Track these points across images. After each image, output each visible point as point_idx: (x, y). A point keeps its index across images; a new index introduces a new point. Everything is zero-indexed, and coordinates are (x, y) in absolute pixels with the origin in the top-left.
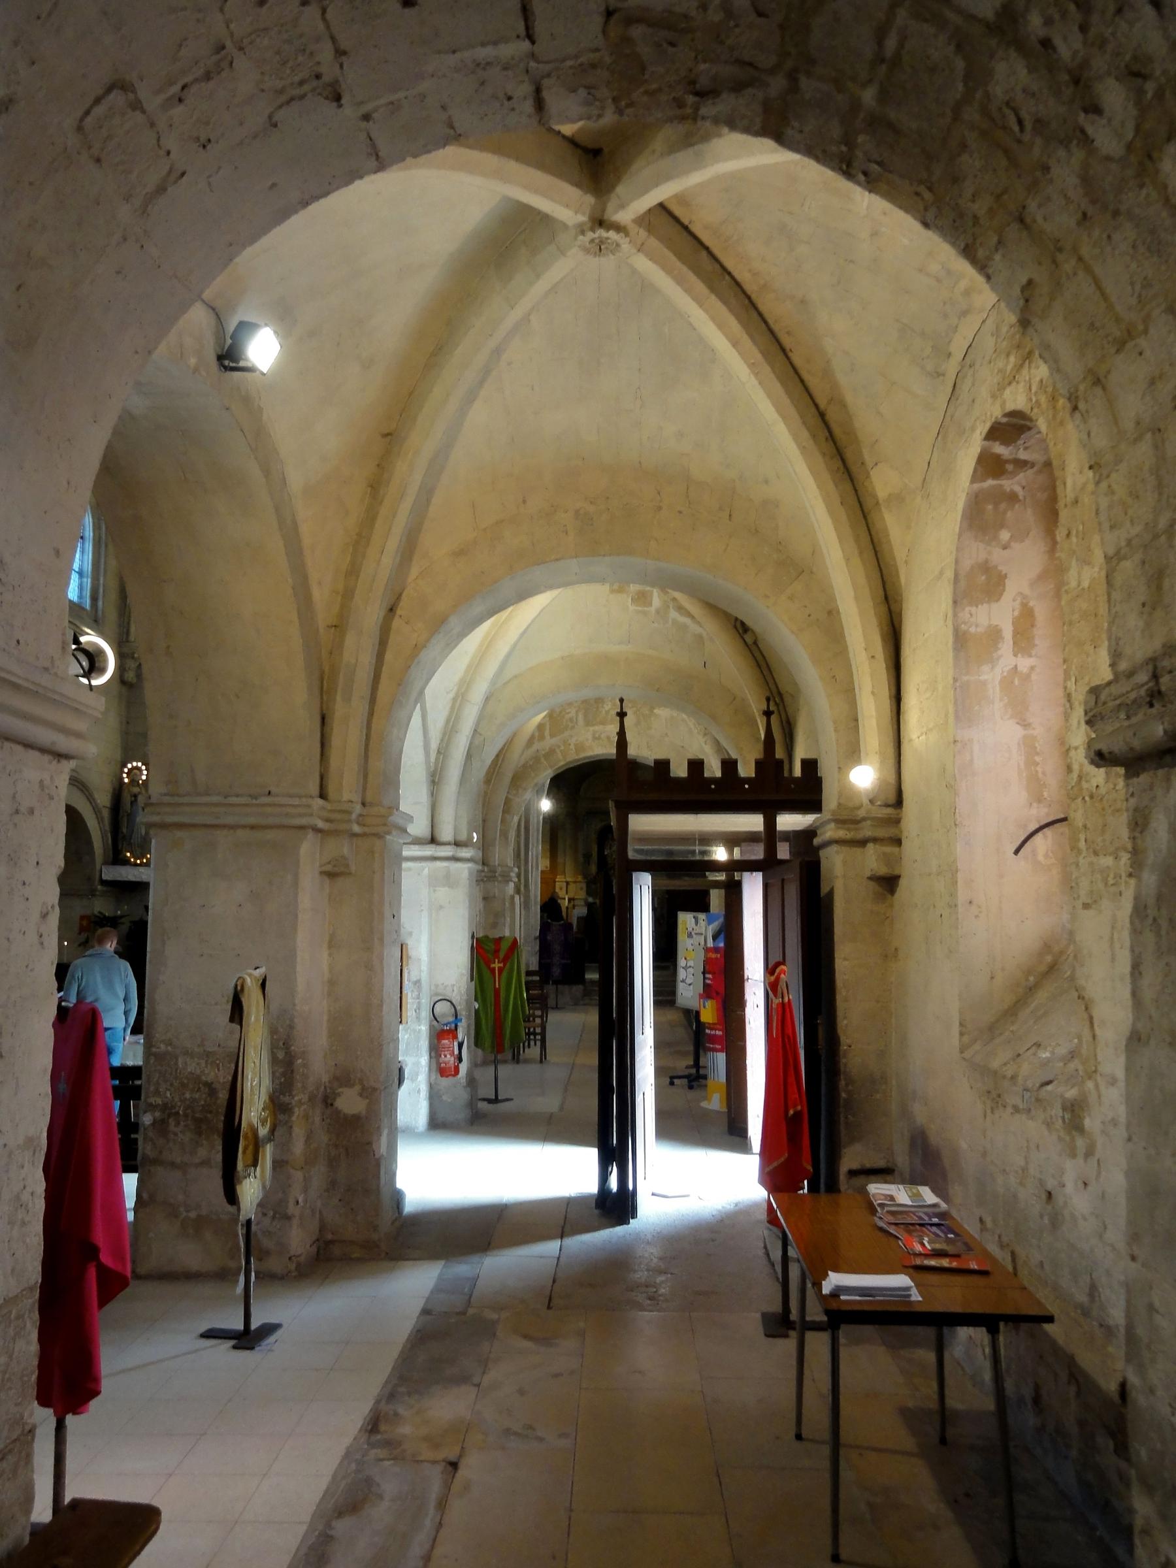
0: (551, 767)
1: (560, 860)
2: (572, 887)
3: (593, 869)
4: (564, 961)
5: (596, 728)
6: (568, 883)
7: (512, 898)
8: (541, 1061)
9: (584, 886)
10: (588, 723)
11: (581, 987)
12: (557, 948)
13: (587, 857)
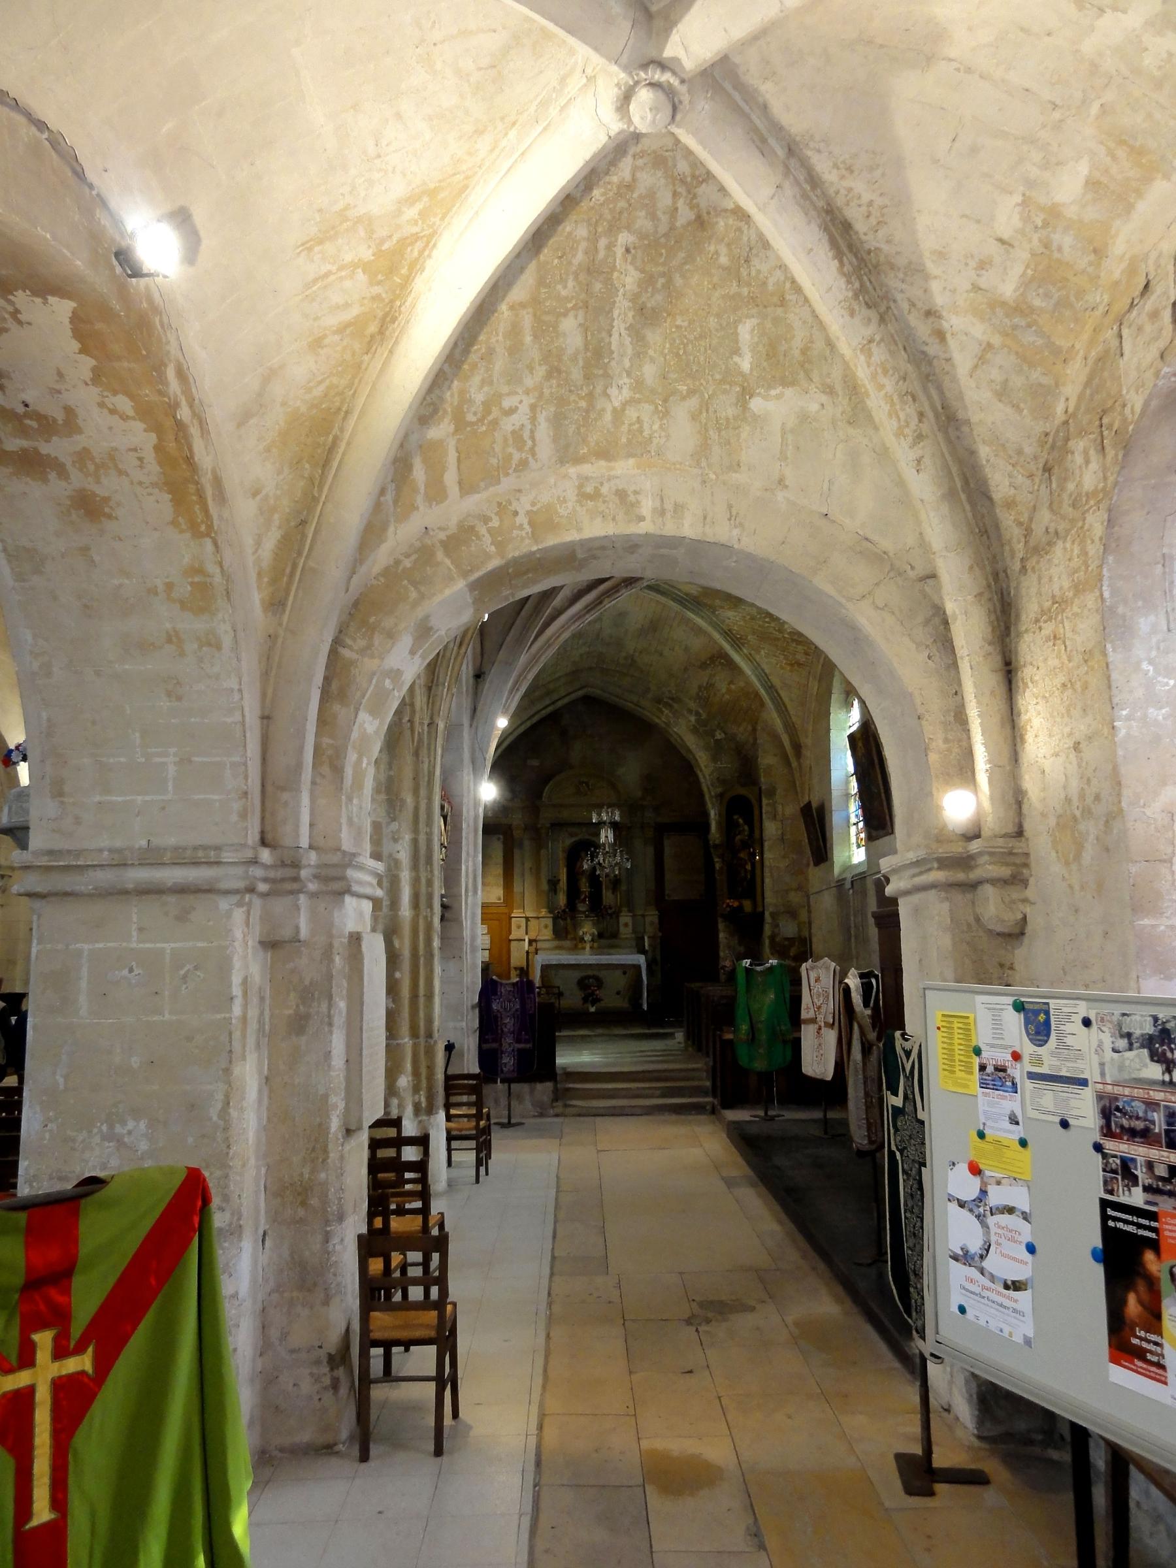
0: (465, 574)
1: (517, 888)
2: (533, 923)
3: (562, 899)
5: (586, 469)
6: (527, 919)
7: (356, 939)
8: (439, 1452)
9: (549, 922)
10: (566, 455)
11: (549, 1085)
12: (509, 1023)
13: (553, 884)
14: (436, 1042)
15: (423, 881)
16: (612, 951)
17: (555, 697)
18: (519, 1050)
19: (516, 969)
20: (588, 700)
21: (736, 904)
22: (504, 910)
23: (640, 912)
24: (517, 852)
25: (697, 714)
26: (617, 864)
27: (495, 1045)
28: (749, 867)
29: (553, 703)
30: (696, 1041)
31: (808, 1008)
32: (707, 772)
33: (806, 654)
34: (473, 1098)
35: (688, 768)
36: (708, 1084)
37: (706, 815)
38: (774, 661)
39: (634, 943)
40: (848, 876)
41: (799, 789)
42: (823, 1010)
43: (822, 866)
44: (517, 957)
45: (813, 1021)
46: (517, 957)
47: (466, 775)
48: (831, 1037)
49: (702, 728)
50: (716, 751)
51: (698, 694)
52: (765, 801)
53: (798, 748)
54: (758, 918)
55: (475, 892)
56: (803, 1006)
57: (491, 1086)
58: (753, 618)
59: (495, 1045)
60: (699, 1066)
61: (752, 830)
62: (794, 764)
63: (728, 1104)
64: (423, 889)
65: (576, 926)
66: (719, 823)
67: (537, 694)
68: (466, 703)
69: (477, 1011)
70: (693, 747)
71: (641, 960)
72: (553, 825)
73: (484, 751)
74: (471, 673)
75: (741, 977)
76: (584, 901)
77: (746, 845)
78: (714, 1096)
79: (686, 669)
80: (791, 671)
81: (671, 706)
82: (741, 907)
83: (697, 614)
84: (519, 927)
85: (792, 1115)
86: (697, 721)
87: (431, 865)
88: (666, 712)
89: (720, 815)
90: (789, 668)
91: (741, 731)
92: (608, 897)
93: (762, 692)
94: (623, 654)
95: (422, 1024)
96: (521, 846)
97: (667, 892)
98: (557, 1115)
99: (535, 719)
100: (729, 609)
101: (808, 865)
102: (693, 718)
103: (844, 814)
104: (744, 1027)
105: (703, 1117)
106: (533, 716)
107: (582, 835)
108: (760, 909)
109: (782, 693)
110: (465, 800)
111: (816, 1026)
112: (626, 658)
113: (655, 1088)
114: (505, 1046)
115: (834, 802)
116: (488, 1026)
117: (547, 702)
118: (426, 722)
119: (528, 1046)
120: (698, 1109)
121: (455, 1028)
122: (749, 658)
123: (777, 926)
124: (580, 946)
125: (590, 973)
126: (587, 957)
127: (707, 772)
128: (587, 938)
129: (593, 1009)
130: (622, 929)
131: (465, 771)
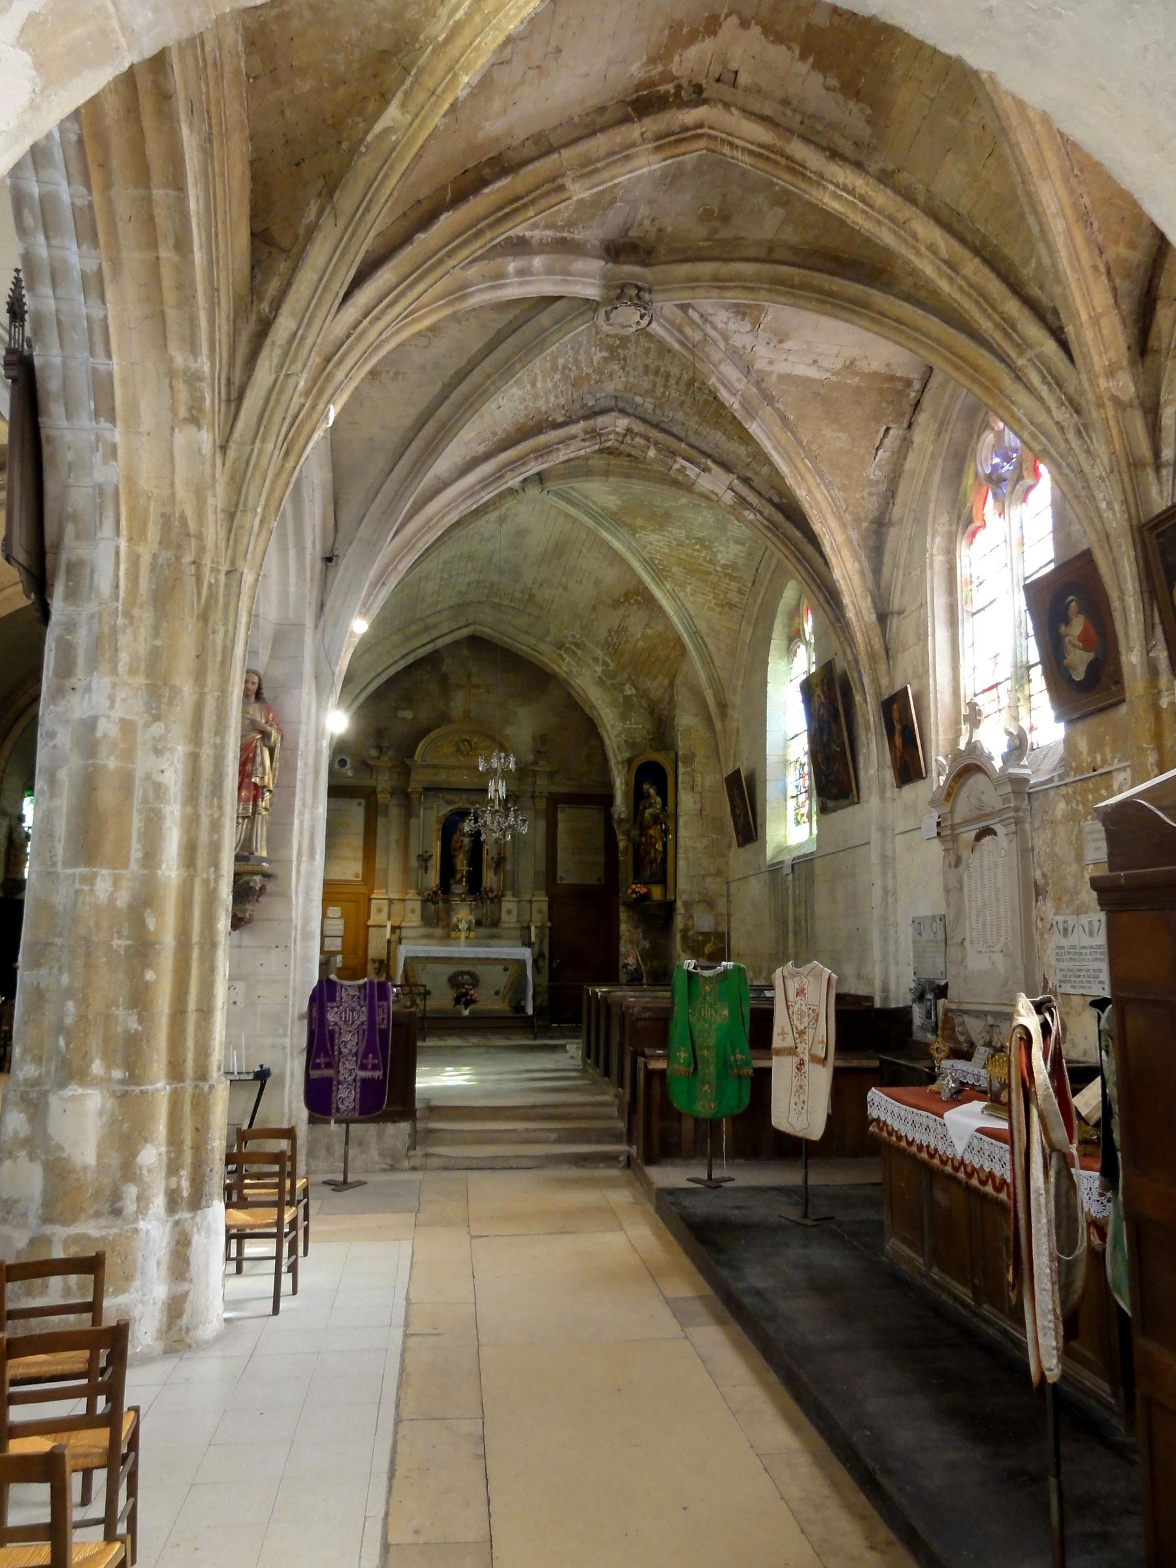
1: (379, 864)
2: (397, 907)
3: (433, 878)
4: (362, 1074)
6: (390, 901)
9: (417, 906)
11: (405, 1126)
12: (349, 1042)
13: (424, 859)
14: (212, 1087)
15: (205, 822)
16: (492, 942)
18: (364, 1081)
19: (374, 961)
20: (475, 641)
21: (643, 890)
22: (363, 890)
23: (528, 897)
24: (381, 821)
25: (605, 663)
26: (510, 826)
27: (329, 1073)
28: (659, 846)
29: (432, 641)
30: (601, 1060)
31: (783, 1033)
32: (613, 733)
33: (740, 592)
34: (276, 1168)
35: (590, 729)
36: (621, 1125)
37: (610, 785)
39: (518, 933)
40: (788, 858)
41: (722, 758)
42: (808, 1037)
43: (748, 847)
44: (376, 947)
45: (792, 1051)
46: (376, 947)
47: (306, 693)
48: (821, 1080)
51: (606, 639)
52: (681, 770)
53: (723, 706)
54: (669, 908)
55: (312, 856)
56: (776, 1030)
57: (327, 1126)
58: (680, 544)
59: (329, 1073)
60: (607, 1098)
61: (665, 803)
62: (718, 727)
63: (650, 1160)
64: (204, 837)
65: (449, 912)
66: (626, 794)
67: (413, 628)
68: (311, 595)
69: (306, 1022)
70: (598, 703)
71: (526, 954)
72: (426, 789)
73: (331, 663)
74: (319, 555)
75: (680, 983)
76: (460, 882)
77: (656, 819)
78: (630, 1142)
79: (594, 608)
80: (721, 613)
81: (574, 653)
82: (646, 897)
83: (614, 535)
84: (380, 911)
85: (745, 1176)
87: (220, 797)
89: (627, 784)
90: (719, 609)
91: (655, 686)
92: (489, 878)
93: (685, 637)
95: (190, 1056)
97: (560, 874)
98: (414, 1169)
99: (410, 659)
100: (653, 531)
101: (730, 846)
102: (599, 669)
103: (780, 785)
104: (683, 1055)
105: (614, 1172)
106: (407, 654)
107: (461, 802)
108: (670, 897)
109: (708, 640)
110: (303, 728)
111: (796, 1060)
112: (523, 591)
113: (550, 1130)
114: (344, 1074)
115: (769, 770)
116: (320, 1043)
117: (425, 639)
118: (224, 567)
119: (378, 1074)
120: (609, 1159)
121: (273, 1046)
122: (673, 596)
123: (691, 917)
124: (453, 934)
125: (465, 968)
126: (461, 949)
127: (613, 733)
128: (463, 926)
129: (466, 1013)
130: (504, 916)
131: (305, 689)
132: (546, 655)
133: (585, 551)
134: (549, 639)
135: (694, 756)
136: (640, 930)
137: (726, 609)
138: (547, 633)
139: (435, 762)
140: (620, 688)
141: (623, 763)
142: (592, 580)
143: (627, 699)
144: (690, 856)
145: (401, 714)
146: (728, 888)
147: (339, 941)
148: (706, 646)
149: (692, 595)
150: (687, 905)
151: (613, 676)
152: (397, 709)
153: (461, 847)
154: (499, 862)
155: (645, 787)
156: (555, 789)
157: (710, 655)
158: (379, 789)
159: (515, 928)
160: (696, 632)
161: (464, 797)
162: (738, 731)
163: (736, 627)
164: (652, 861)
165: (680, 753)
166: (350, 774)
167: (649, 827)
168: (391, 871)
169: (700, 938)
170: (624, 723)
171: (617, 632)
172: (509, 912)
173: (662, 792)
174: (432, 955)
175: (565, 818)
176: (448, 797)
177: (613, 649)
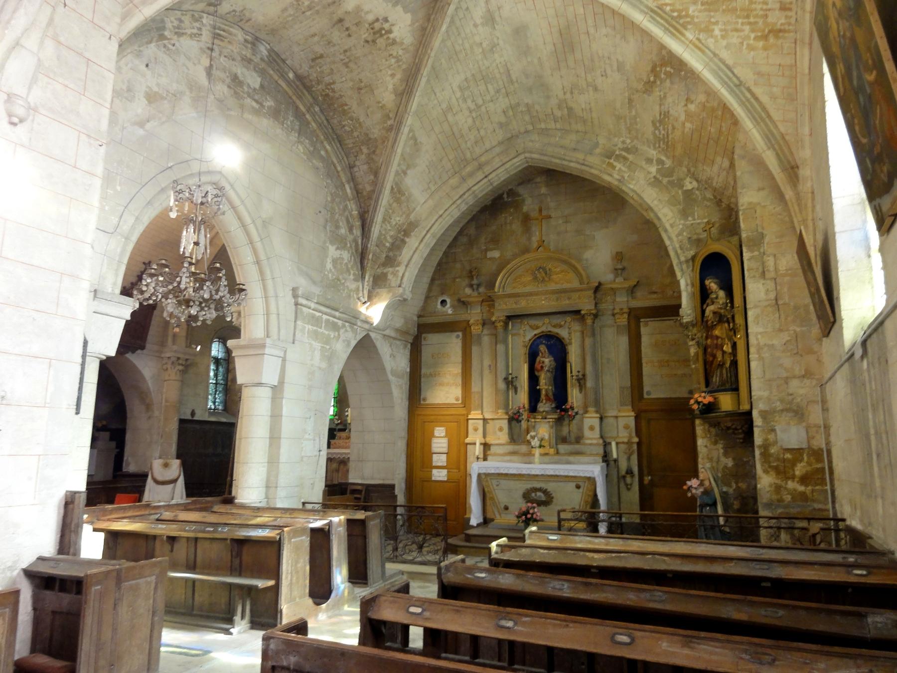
1: (475, 388)
3: (522, 398)
9: (505, 424)
13: (510, 383)
16: (571, 458)
17: (487, 169)
21: (708, 399)
24: (475, 350)
25: (660, 162)
28: (727, 348)
38: (734, 39)
49: (665, 180)
50: (687, 203)
51: (654, 134)
52: (746, 255)
53: (792, 170)
62: (789, 194)
67: (469, 169)
71: (595, 470)
72: (509, 318)
77: (721, 318)
79: (630, 101)
80: (765, 49)
81: (625, 159)
84: (476, 430)
86: (658, 171)
88: (618, 166)
89: (693, 285)
90: (761, 44)
91: (715, 172)
92: (574, 396)
93: (725, 93)
94: (554, 102)
96: (479, 343)
97: (646, 389)
102: (653, 169)
107: (545, 326)
108: (745, 407)
109: (758, 91)
112: (560, 107)
117: (480, 175)
122: (699, 47)
123: (773, 430)
126: (538, 467)
127: (673, 232)
130: (587, 433)
132: (594, 166)
133: (592, 31)
134: (598, 151)
135: (762, 236)
136: (720, 446)
137: (772, 40)
138: (597, 145)
139: (513, 291)
140: (680, 184)
141: (687, 261)
142: (615, 67)
143: (688, 194)
144: (766, 355)
145: (490, 254)
146: (823, 392)
147: (444, 457)
148: (756, 99)
149: (723, 37)
150: (764, 415)
151: (669, 173)
152: (486, 250)
153: (542, 367)
154: (581, 381)
155: (707, 282)
156: (635, 304)
157: (764, 109)
158: (471, 322)
159: (597, 444)
160: (740, 84)
161: (547, 320)
162: (813, 193)
163: (789, 61)
164: (721, 365)
165: (744, 235)
166: (450, 312)
167: (713, 327)
168: (485, 394)
169: (788, 456)
170: (686, 218)
171: (660, 121)
172: (592, 428)
173: (728, 288)
174: (502, 471)
175: (649, 331)
176: (533, 322)
177: (664, 143)
